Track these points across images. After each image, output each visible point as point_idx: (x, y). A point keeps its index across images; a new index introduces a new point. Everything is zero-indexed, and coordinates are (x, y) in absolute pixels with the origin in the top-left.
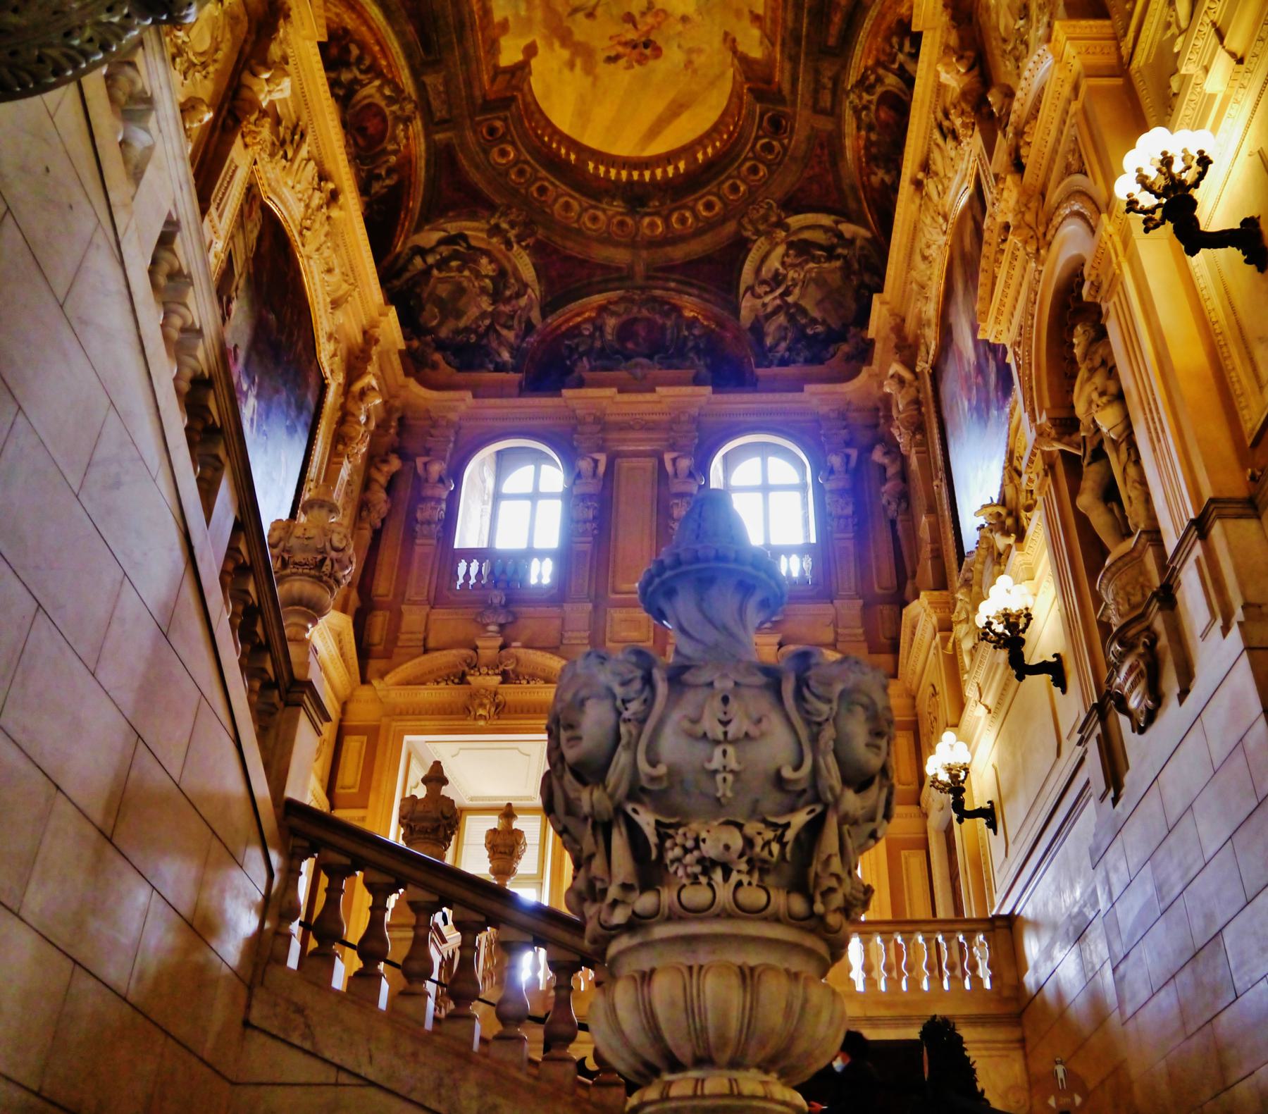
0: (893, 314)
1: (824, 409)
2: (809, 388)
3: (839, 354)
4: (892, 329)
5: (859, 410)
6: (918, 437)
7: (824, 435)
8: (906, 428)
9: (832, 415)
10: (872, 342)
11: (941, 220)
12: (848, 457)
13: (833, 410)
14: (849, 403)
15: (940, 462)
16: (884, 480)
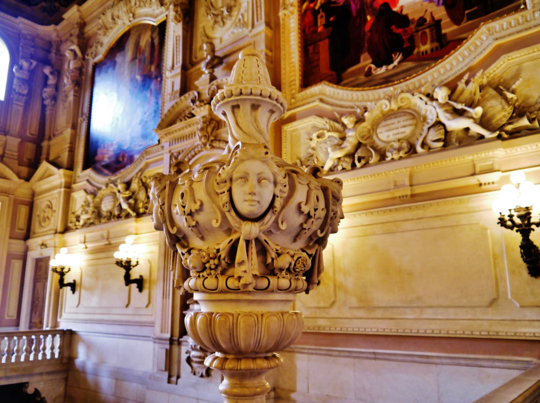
0: (81, 17)
1: (25, 32)
2: (20, 19)
3: (39, 6)
4: (77, 23)
5: (42, 39)
6: (76, 88)
7: (22, 47)
8: (71, 79)
9: (28, 37)
10: (63, 19)
11: (131, 15)
12: (31, 63)
13: (29, 35)
14: (38, 34)
15: (86, 110)
16: (45, 85)
